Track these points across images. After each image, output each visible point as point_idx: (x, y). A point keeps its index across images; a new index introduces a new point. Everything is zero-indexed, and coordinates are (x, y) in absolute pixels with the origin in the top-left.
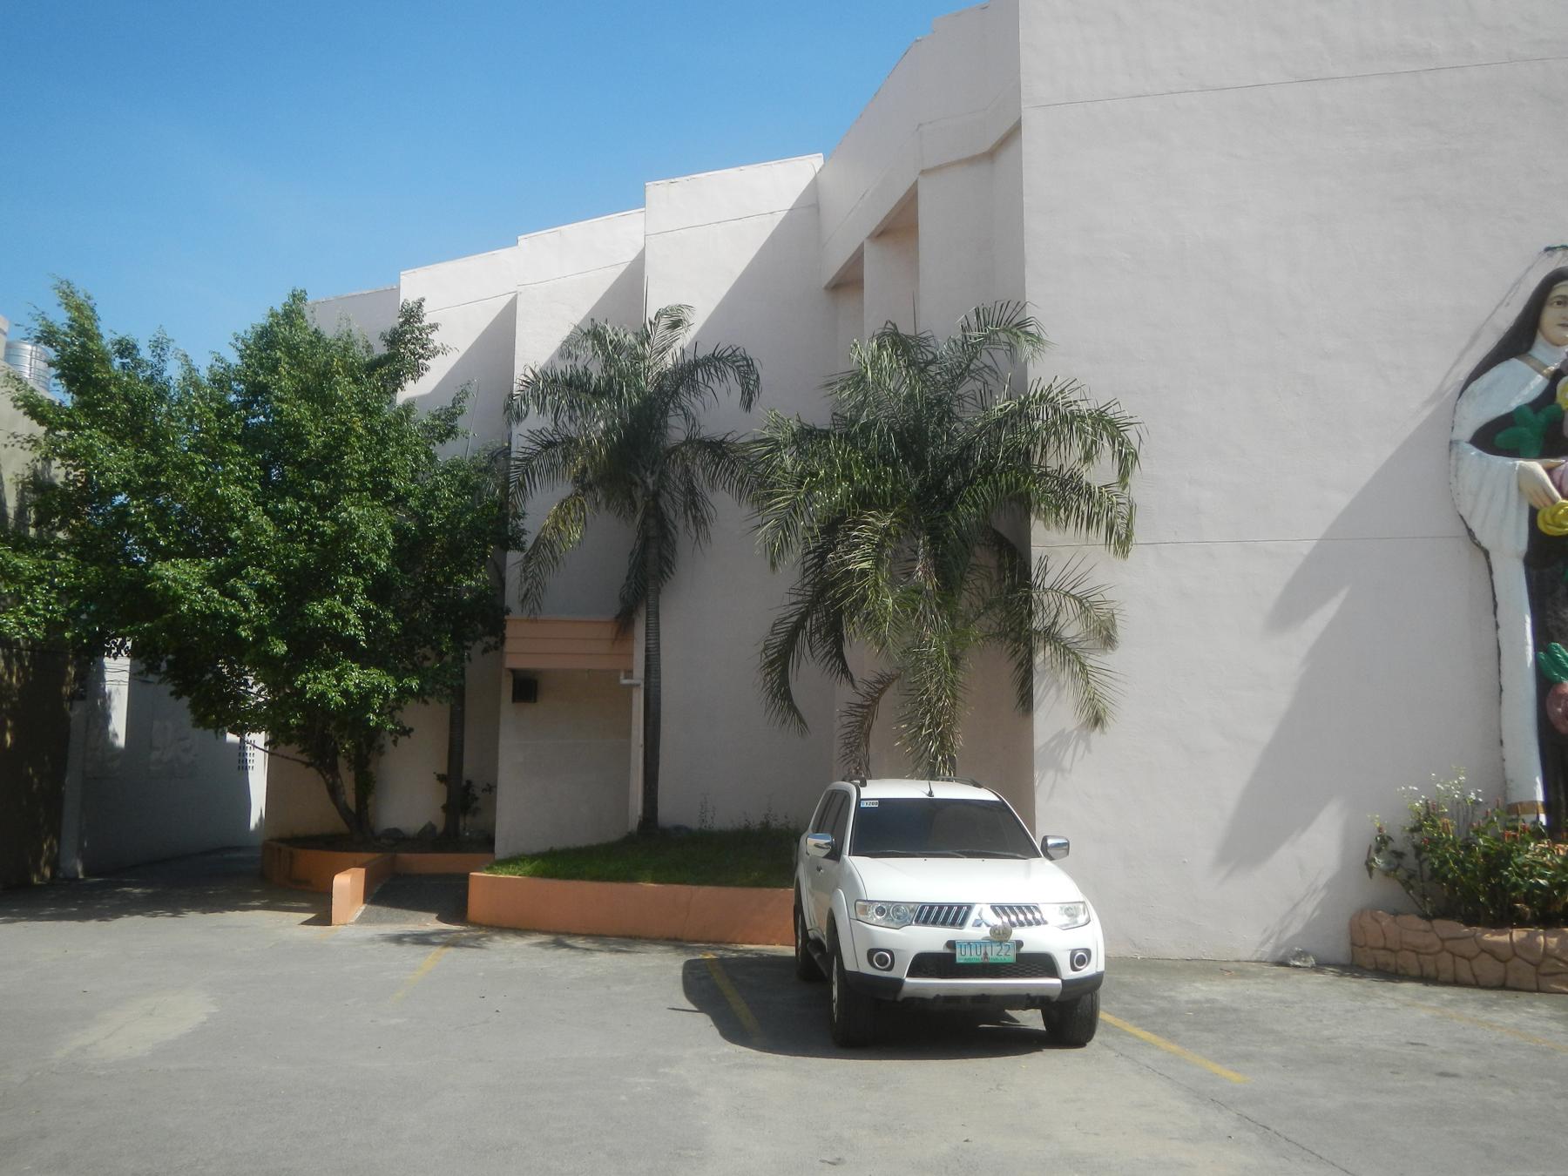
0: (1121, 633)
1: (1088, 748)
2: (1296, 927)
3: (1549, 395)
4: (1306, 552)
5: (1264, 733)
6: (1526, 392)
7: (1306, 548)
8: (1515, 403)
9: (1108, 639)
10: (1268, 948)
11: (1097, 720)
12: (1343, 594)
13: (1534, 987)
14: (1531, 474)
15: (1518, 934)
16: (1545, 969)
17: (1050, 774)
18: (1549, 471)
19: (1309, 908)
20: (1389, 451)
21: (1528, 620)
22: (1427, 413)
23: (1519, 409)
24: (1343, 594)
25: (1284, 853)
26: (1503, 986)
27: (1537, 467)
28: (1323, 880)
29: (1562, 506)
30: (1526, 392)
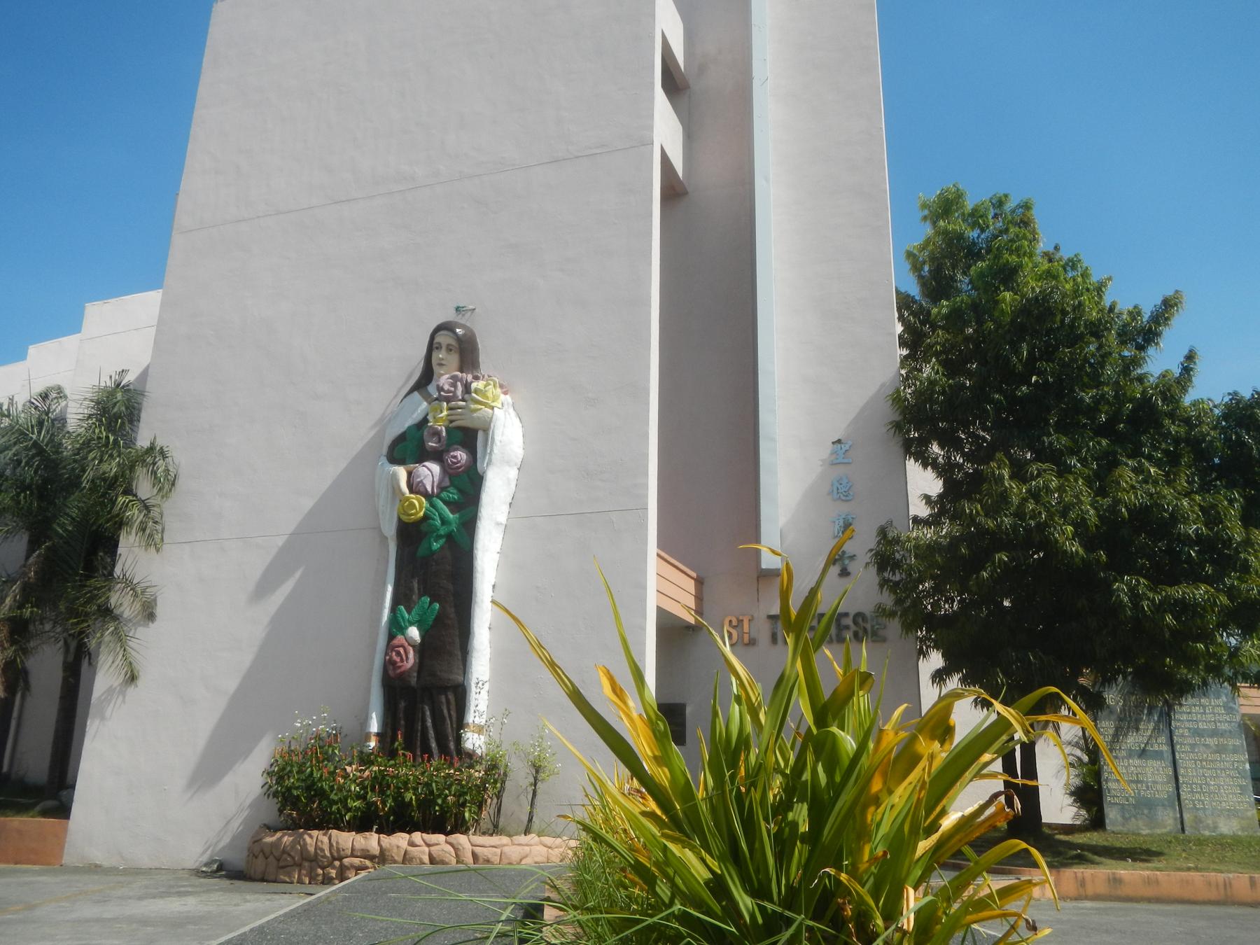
0: (159, 611)
1: (124, 701)
2: (226, 840)
3: (425, 421)
4: (280, 543)
5: (231, 685)
6: (415, 416)
7: (280, 542)
8: (407, 426)
9: (150, 616)
10: (205, 858)
11: (132, 678)
12: (298, 574)
13: (272, 877)
14: (394, 478)
15: (279, 834)
16: (282, 864)
17: (97, 722)
18: (410, 474)
19: (236, 825)
20: (343, 465)
21: (390, 589)
22: (372, 433)
23: (409, 428)
24: (298, 574)
25: (228, 780)
26: (263, 880)
27: (402, 472)
28: (249, 801)
29: (408, 499)
30: (415, 416)
